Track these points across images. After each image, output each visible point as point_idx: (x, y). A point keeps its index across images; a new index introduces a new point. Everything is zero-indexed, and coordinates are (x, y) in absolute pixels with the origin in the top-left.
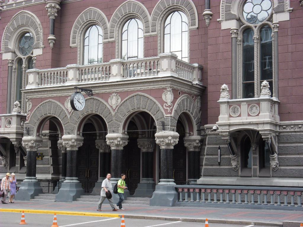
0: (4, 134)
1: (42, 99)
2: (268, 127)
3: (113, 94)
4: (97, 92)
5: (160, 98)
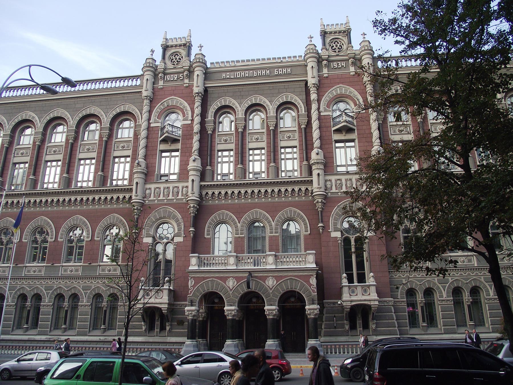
1: (204, 278)
2: (377, 303)
3: (270, 277)
4: (256, 275)
5: (308, 282)
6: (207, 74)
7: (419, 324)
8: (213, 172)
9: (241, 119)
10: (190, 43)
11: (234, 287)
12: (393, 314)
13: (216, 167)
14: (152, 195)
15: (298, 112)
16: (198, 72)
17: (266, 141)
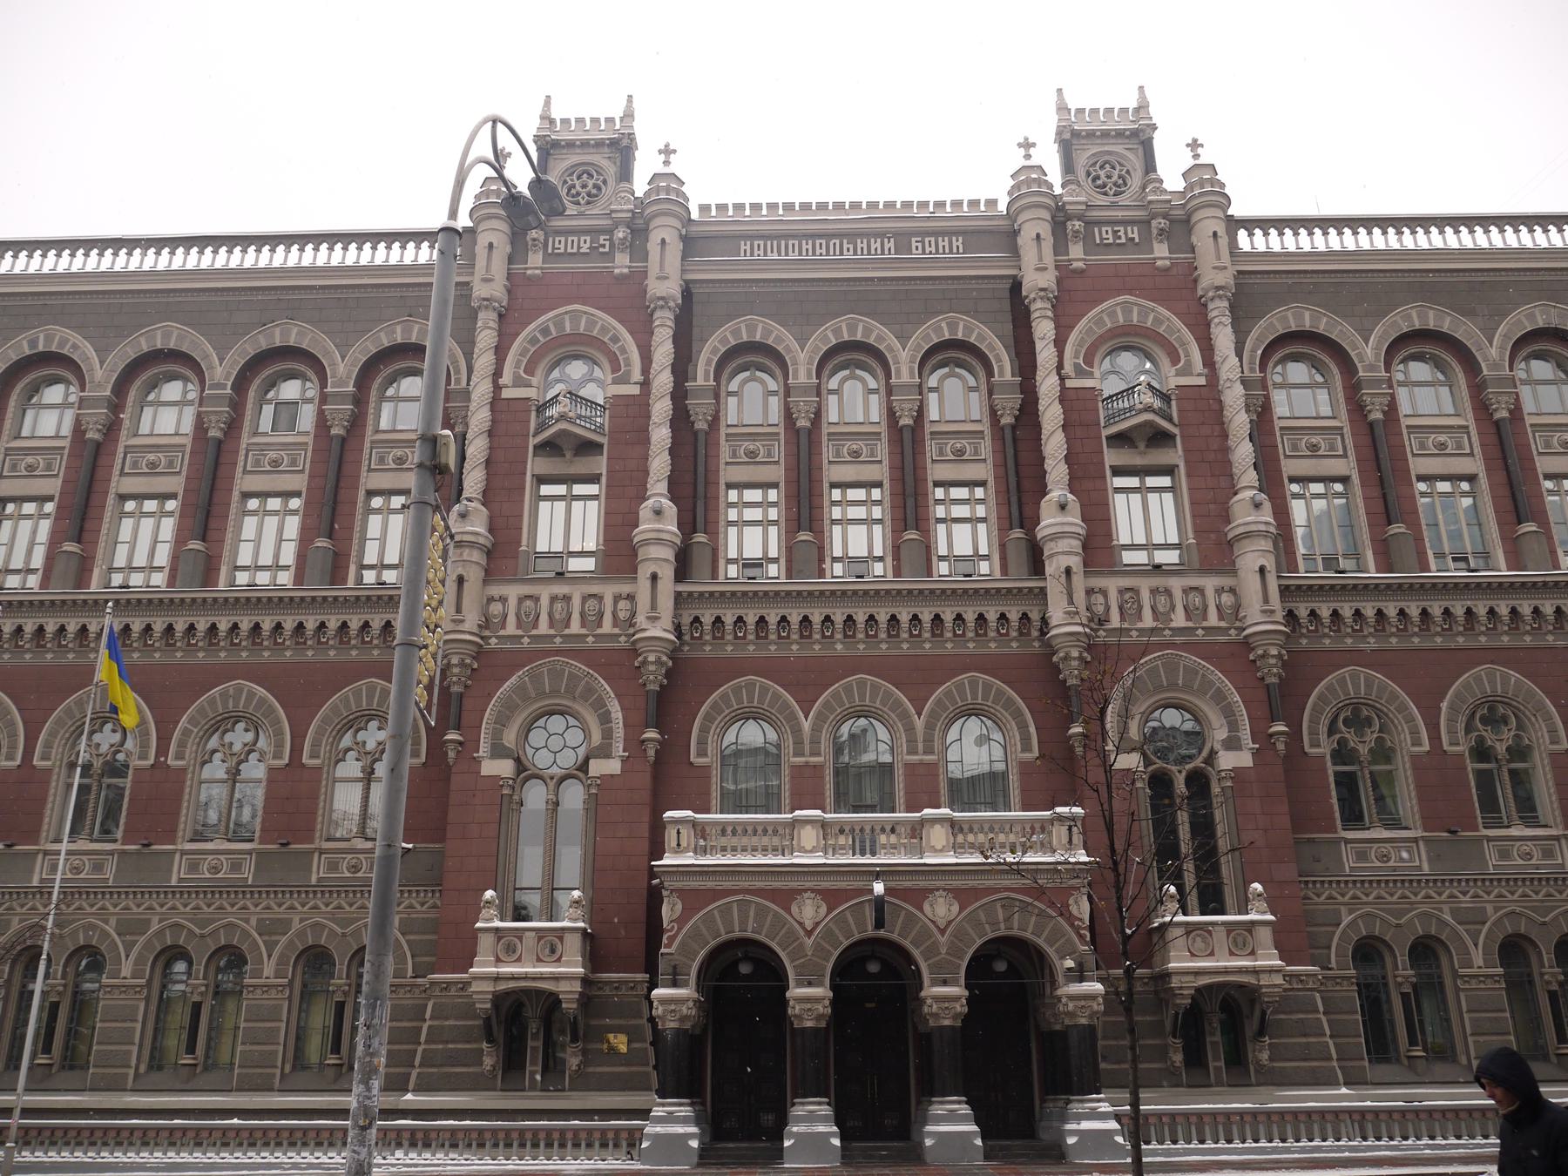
0: (534, 979)
1: (717, 894)
6: (694, 241)
7: (1397, 1050)
8: (715, 551)
9: (805, 390)
10: (631, 137)
11: (818, 924)
12: (1322, 1016)
13: (721, 536)
14: (511, 619)
15: (990, 374)
16: (664, 232)
17: (886, 462)
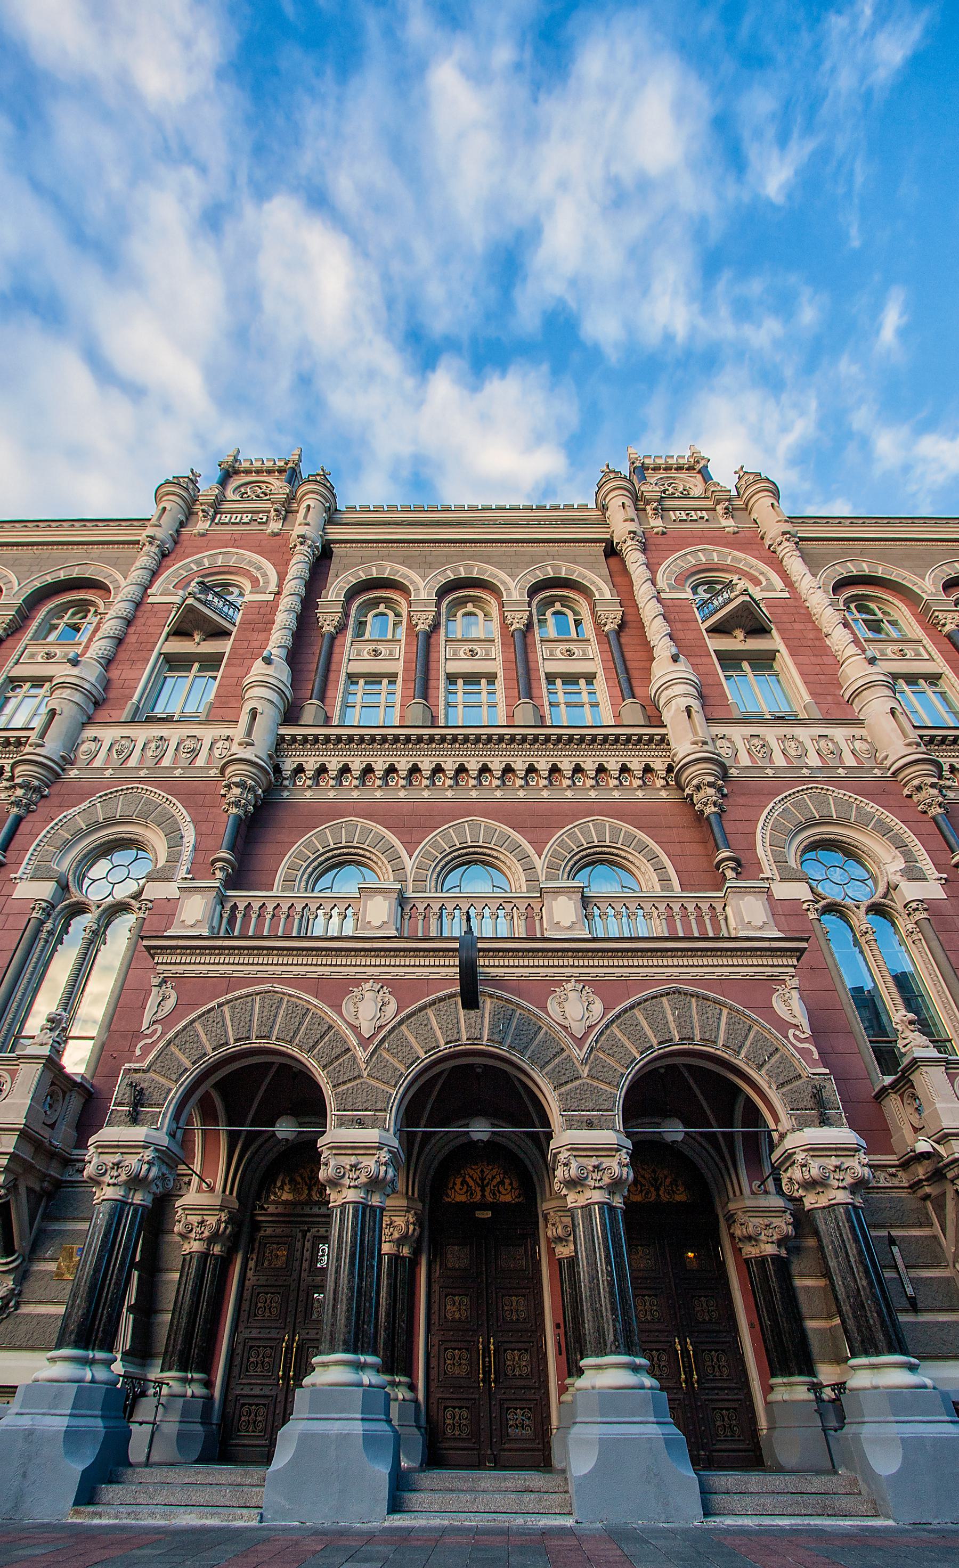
1: (231, 983)
11: (381, 1027)
17: (500, 658)
